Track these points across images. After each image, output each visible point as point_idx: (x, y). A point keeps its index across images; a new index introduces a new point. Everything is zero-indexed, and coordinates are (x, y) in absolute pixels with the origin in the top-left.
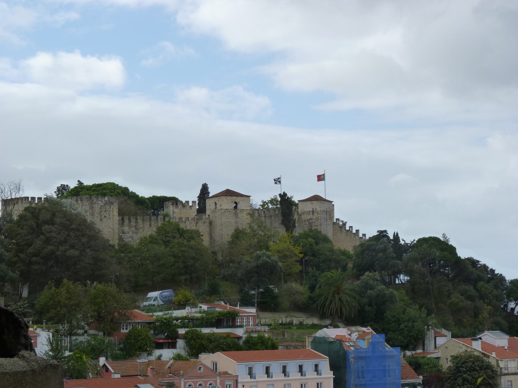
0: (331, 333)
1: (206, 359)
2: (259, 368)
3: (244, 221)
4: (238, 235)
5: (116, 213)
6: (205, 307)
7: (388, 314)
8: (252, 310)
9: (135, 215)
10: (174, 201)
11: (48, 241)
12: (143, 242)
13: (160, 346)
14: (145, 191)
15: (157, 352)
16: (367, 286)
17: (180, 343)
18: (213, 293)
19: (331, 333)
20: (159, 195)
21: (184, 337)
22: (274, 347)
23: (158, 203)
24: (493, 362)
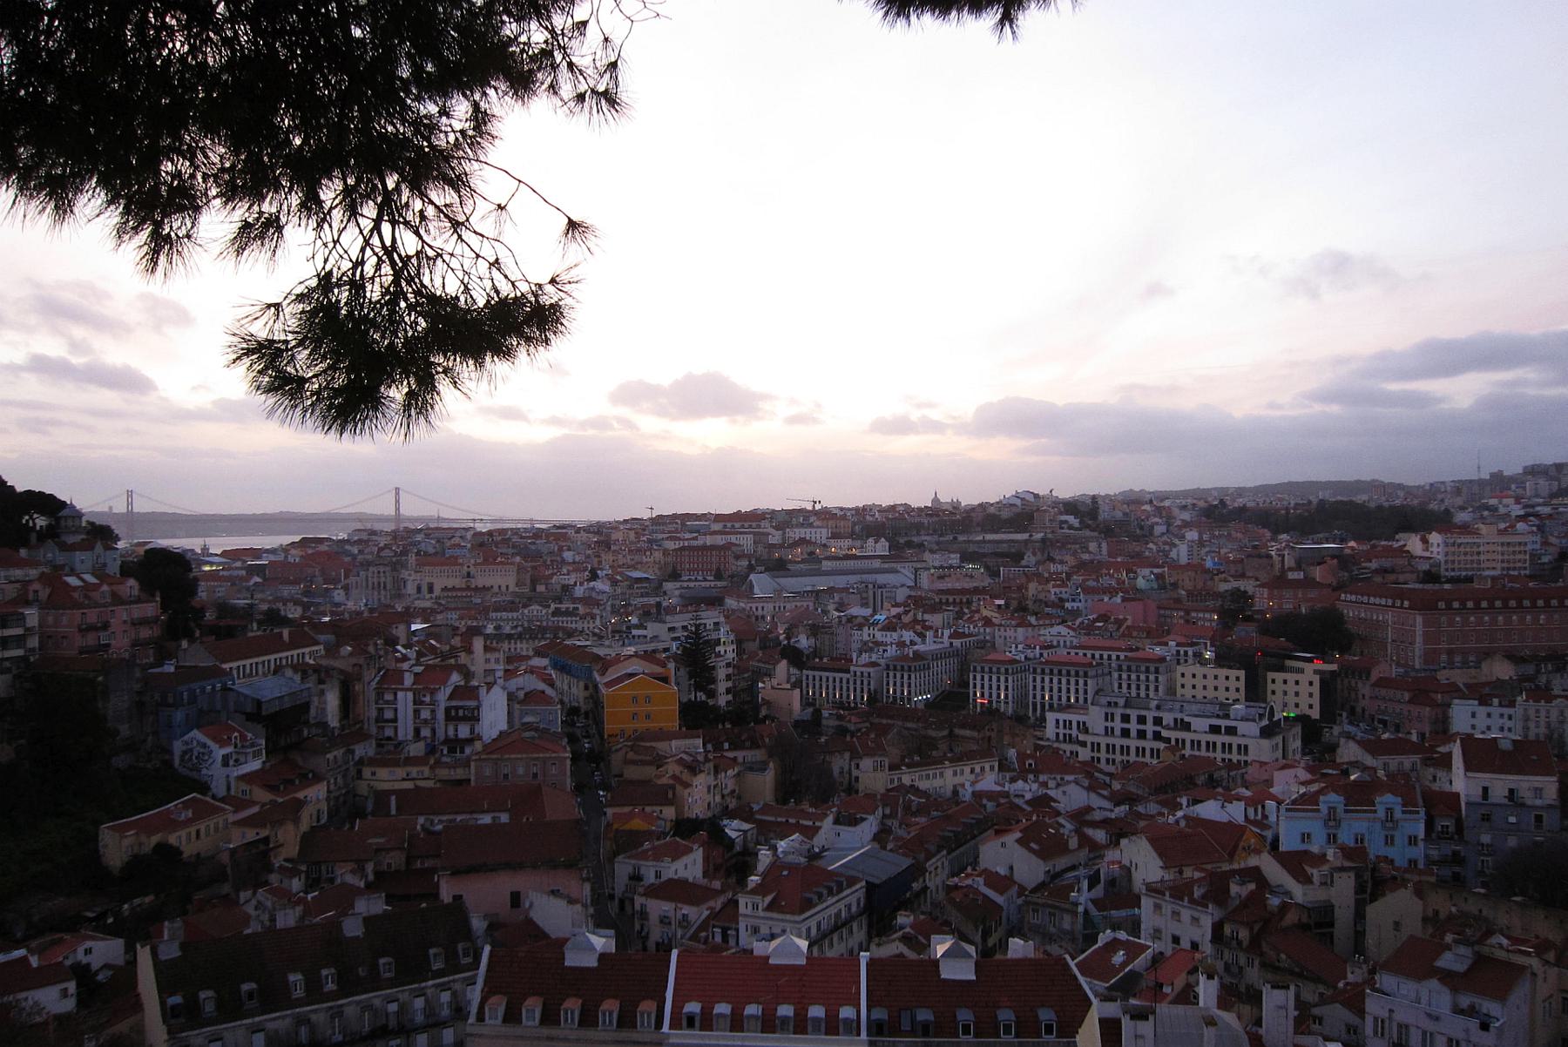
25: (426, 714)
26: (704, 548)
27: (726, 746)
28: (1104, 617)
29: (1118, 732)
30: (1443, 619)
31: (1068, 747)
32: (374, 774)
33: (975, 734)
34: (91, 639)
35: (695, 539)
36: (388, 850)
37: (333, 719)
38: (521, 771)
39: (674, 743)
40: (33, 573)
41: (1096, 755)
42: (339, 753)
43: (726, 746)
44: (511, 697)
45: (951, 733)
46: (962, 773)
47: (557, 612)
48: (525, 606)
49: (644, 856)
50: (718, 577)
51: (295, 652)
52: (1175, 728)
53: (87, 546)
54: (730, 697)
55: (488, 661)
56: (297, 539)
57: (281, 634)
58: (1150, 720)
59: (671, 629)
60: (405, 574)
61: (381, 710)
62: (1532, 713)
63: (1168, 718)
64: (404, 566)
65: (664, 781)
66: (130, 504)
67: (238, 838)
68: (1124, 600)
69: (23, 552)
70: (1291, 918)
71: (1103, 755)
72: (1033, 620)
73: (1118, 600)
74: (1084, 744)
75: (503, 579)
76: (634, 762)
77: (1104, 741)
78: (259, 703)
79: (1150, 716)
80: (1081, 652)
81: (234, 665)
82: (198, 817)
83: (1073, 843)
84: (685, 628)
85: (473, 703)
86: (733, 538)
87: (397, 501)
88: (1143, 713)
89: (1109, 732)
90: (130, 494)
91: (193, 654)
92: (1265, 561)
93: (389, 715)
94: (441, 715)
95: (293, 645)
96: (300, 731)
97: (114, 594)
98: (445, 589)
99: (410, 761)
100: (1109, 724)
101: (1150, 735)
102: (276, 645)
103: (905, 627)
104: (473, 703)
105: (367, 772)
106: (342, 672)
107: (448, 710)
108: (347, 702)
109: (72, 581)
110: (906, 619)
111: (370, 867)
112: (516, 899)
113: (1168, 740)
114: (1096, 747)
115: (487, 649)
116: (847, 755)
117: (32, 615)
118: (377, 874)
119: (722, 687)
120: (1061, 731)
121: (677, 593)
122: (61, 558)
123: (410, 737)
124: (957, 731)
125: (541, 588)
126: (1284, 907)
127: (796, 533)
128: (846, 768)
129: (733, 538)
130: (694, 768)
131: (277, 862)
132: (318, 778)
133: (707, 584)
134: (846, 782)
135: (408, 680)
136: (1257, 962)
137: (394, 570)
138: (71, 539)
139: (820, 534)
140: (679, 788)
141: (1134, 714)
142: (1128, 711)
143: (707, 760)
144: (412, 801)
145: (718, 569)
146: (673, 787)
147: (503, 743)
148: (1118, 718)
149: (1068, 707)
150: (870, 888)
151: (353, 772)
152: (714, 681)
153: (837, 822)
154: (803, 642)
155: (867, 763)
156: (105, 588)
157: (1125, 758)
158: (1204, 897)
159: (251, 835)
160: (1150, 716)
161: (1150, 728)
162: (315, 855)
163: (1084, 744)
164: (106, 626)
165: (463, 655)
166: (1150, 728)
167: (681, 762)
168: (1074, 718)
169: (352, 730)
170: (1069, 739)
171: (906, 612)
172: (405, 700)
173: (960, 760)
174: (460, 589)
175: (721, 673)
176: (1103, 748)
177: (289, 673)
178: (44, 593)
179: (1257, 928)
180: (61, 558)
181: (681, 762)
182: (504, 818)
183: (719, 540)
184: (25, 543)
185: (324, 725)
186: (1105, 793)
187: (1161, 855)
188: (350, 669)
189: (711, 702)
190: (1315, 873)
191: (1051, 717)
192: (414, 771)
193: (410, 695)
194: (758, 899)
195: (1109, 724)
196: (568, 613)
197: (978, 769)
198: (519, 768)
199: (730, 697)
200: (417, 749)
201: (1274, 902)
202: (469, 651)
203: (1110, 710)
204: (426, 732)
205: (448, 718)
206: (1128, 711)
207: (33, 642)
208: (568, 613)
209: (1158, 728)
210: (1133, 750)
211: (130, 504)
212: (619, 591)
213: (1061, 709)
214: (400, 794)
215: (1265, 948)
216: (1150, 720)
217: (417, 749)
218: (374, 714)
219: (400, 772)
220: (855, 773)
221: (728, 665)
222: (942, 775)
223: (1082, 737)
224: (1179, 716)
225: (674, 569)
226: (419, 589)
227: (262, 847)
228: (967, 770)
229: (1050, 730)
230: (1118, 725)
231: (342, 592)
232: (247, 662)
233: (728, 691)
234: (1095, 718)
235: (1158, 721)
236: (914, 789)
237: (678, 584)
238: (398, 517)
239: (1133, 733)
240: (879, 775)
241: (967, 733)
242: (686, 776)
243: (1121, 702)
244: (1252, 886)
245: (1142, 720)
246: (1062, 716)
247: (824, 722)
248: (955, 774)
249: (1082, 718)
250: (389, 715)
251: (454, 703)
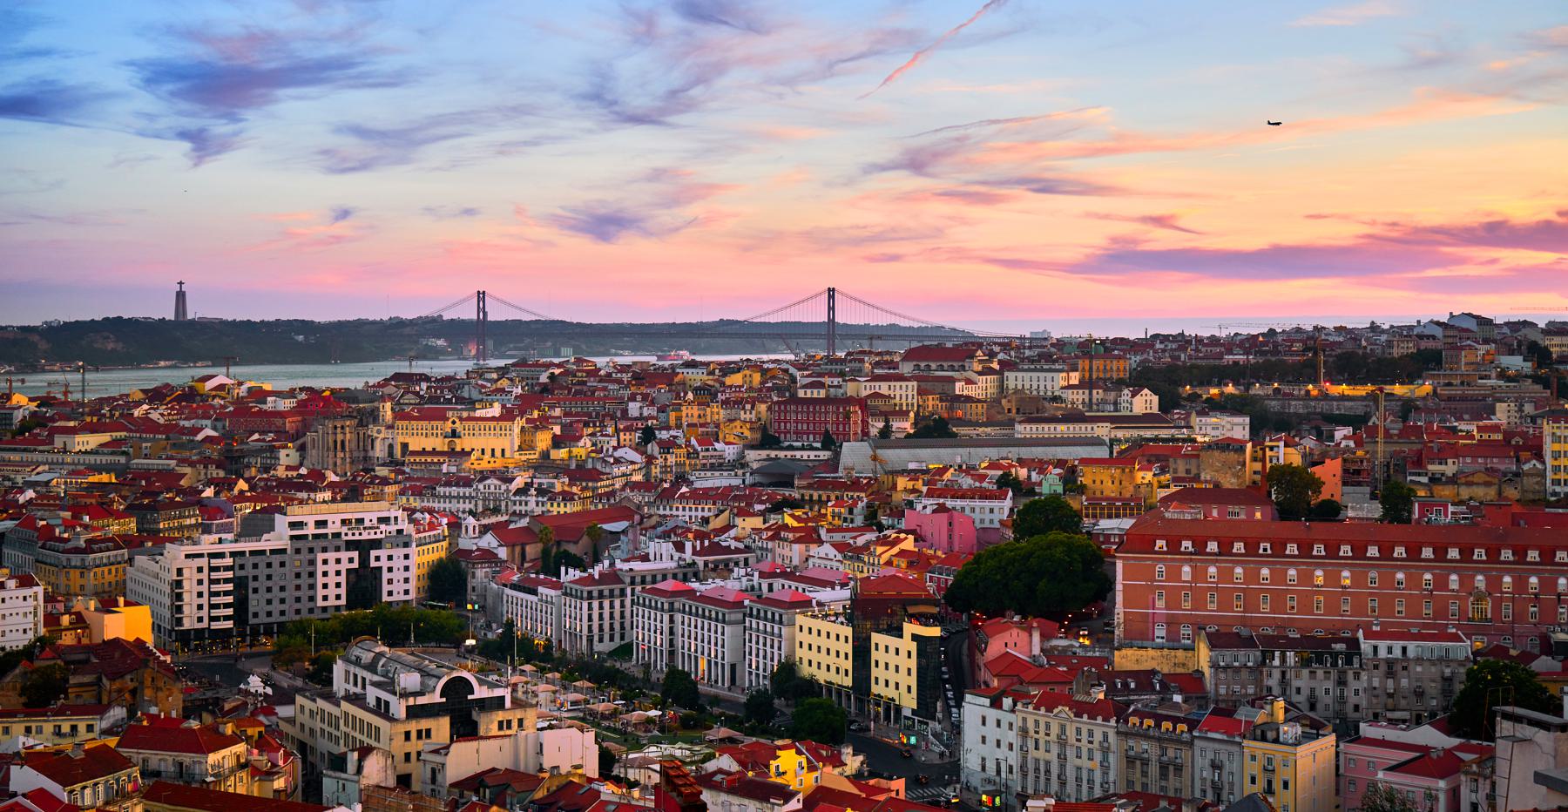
30: (1160, 567)
46: (40, 731)
48: (481, 481)
60: (373, 430)
62: (1031, 725)
66: (482, 309)
86: (883, 388)
87: (831, 309)
90: (481, 296)
92: (1232, 456)
129: (883, 388)
133: (812, 454)
137: (361, 424)
174: (442, 453)
197: (66, 728)
211: (482, 309)
228: (48, 728)
238: (831, 330)
248: (28, 730)
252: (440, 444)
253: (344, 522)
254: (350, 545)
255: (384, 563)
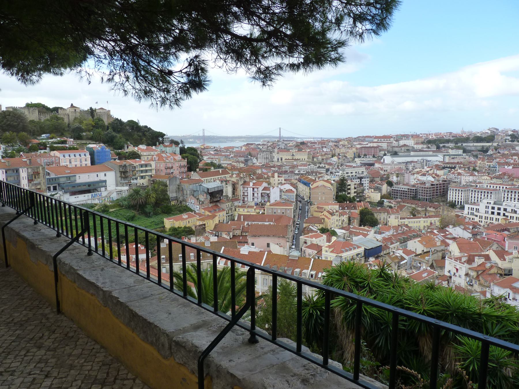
0: (91, 146)
1: (53, 153)
2: (77, 155)
3: (78, 115)
4: (76, 119)
5: (37, 112)
6: (59, 139)
7: (114, 141)
8: (72, 140)
9: (45, 113)
10: (61, 108)
11: (8, 121)
12: (45, 121)
13: (41, 149)
14: (51, 106)
15: (39, 151)
16: (108, 133)
17: (48, 148)
18: (62, 135)
19: (91, 146)
20: (57, 106)
21: (48, 147)
22: (77, 149)
23: (56, 109)
24: (139, 153)
25: (256, 195)
26: (370, 147)
27: (346, 208)
28: (504, 174)
29: (490, 213)
31: (472, 217)
32: (239, 210)
33: (434, 210)
34: (168, 171)
35: (367, 144)
36: (237, 229)
37: (230, 195)
38: (279, 211)
39: (329, 206)
40: (156, 153)
41: (481, 220)
42: (230, 204)
43: (346, 208)
44: (281, 191)
45: (426, 210)
47: (319, 167)
48: (309, 165)
49: (307, 237)
50: (374, 157)
51: (223, 176)
52: (512, 212)
53: (170, 146)
54: (356, 194)
55: (279, 180)
56: (246, 143)
57: (219, 171)
58: (502, 209)
59: (347, 173)
60: (274, 154)
61: (244, 193)
63: (509, 209)
64: (274, 152)
65: (323, 217)
66: (204, 133)
67: (199, 223)
68: (513, 168)
69: (154, 147)
70: (493, 271)
71: (483, 220)
72: (476, 174)
73: (511, 167)
74: (477, 216)
75: (303, 156)
76: (317, 211)
77: (484, 215)
78: (208, 189)
79: (502, 208)
80: (492, 186)
81: (205, 179)
82: (189, 218)
83: (439, 244)
84: (352, 173)
85: (268, 192)
86: (380, 144)
87: (280, 132)
88: (499, 206)
89: (487, 212)
91: (194, 176)
93: (246, 194)
94: (260, 195)
95: (222, 174)
96: (220, 197)
97: (175, 159)
98: (286, 159)
99: (249, 207)
100: (487, 210)
101: (502, 214)
102: (217, 173)
103: (429, 174)
104: (268, 192)
105: (237, 209)
106: (233, 182)
107: (262, 194)
108: (234, 189)
109: (164, 155)
110: (430, 172)
111: (231, 234)
112: (268, 245)
113: (507, 216)
114: (481, 217)
115: (278, 177)
116: (386, 214)
117: (153, 163)
118: (234, 236)
119: (352, 191)
120: (470, 211)
121: (359, 162)
122: (164, 149)
123: (252, 200)
124: (428, 209)
125: (315, 160)
126: (492, 267)
127: (402, 143)
128: (386, 218)
129: (380, 144)
130: (332, 214)
131: (207, 229)
132: (223, 210)
134: (385, 222)
135: (251, 184)
136: (478, 283)
138: (166, 144)
139: (410, 143)
140: (326, 219)
141: (496, 207)
142: (494, 206)
143: (337, 212)
144: (247, 217)
145: (374, 155)
146: (324, 219)
147: (277, 204)
148: (490, 208)
149: (474, 204)
150: (365, 249)
151: (233, 209)
152: (349, 189)
153: (375, 233)
154: (394, 179)
155: (393, 217)
156: (172, 157)
157: (491, 221)
158: (465, 262)
159: (201, 223)
160: (502, 208)
161: (502, 212)
162: (217, 230)
163: (477, 216)
164: (172, 168)
165: (271, 178)
166: (502, 212)
167: (328, 212)
168: (475, 207)
169: (235, 197)
170: (472, 214)
171: (431, 170)
172: (250, 190)
173: (427, 218)
175: (352, 187)
176: (484, 218)
177: (218, 181)
178: (157, 159)
179: (480, 273)
180: (164, 149)
181: (328, 212)
182: (272, 223)
183: (375, 145)
184: (155, 145)
185: (227, 196)
186: (469, 231)
187: (459, 249)
188: (235, 181)
189: (348, 195)
190: (506, 257)
191: (466, 206)
192: (250, 210)
193: (252, 189)
194: (327, 249)
195: (487, 210)
196: (322, 168)
198: (279, 210)
199: (356, 194)
200: (253, 204)
201: (488, 265)
202: (273, 177)
203: (487, 205)
204: (256, 200)
205: (262, 196)
206: (494, 206)
207: (154, 172)
208: (322, 168)
209: (504, 212)
210: (494, 219)
211: (204, 133)
212: (340, 161)
213: (471, 204)
214: (243, 215)
215: (481, 278)
216: (502, 209)
217: (253, 204)
218: (242, 194)
219: (246, 210)
220: (388, 219)
221: (355, 184)
222: (419, 222)
223: (476, 213)
224: (513, 208)
225: (359, 154)
226: (278, 159)
227: (204, 226)
229: (466, 211)
230: (490, 210)
231: (256, 160)
232: (209, 178)
233: (355, 192)
234: (482, 207)
235: (505, 210)
236: (407, 226)
237: (360, 159)
238: (280, 137)
239: (496, 213)
240: (397, 220)
241: (432, 209)
242: (329, 216)
243: (492, 202)
244: (483, 260)
245: (499, 209)
246: (471, 206)
247: (385, 203)
248: (424, 222)
249: (477, 207)
250: (246, 194)
251: (263, 192)
252: (290, 157)
253: (356, 172)
254: (358, 178)
255: (364, 182)
